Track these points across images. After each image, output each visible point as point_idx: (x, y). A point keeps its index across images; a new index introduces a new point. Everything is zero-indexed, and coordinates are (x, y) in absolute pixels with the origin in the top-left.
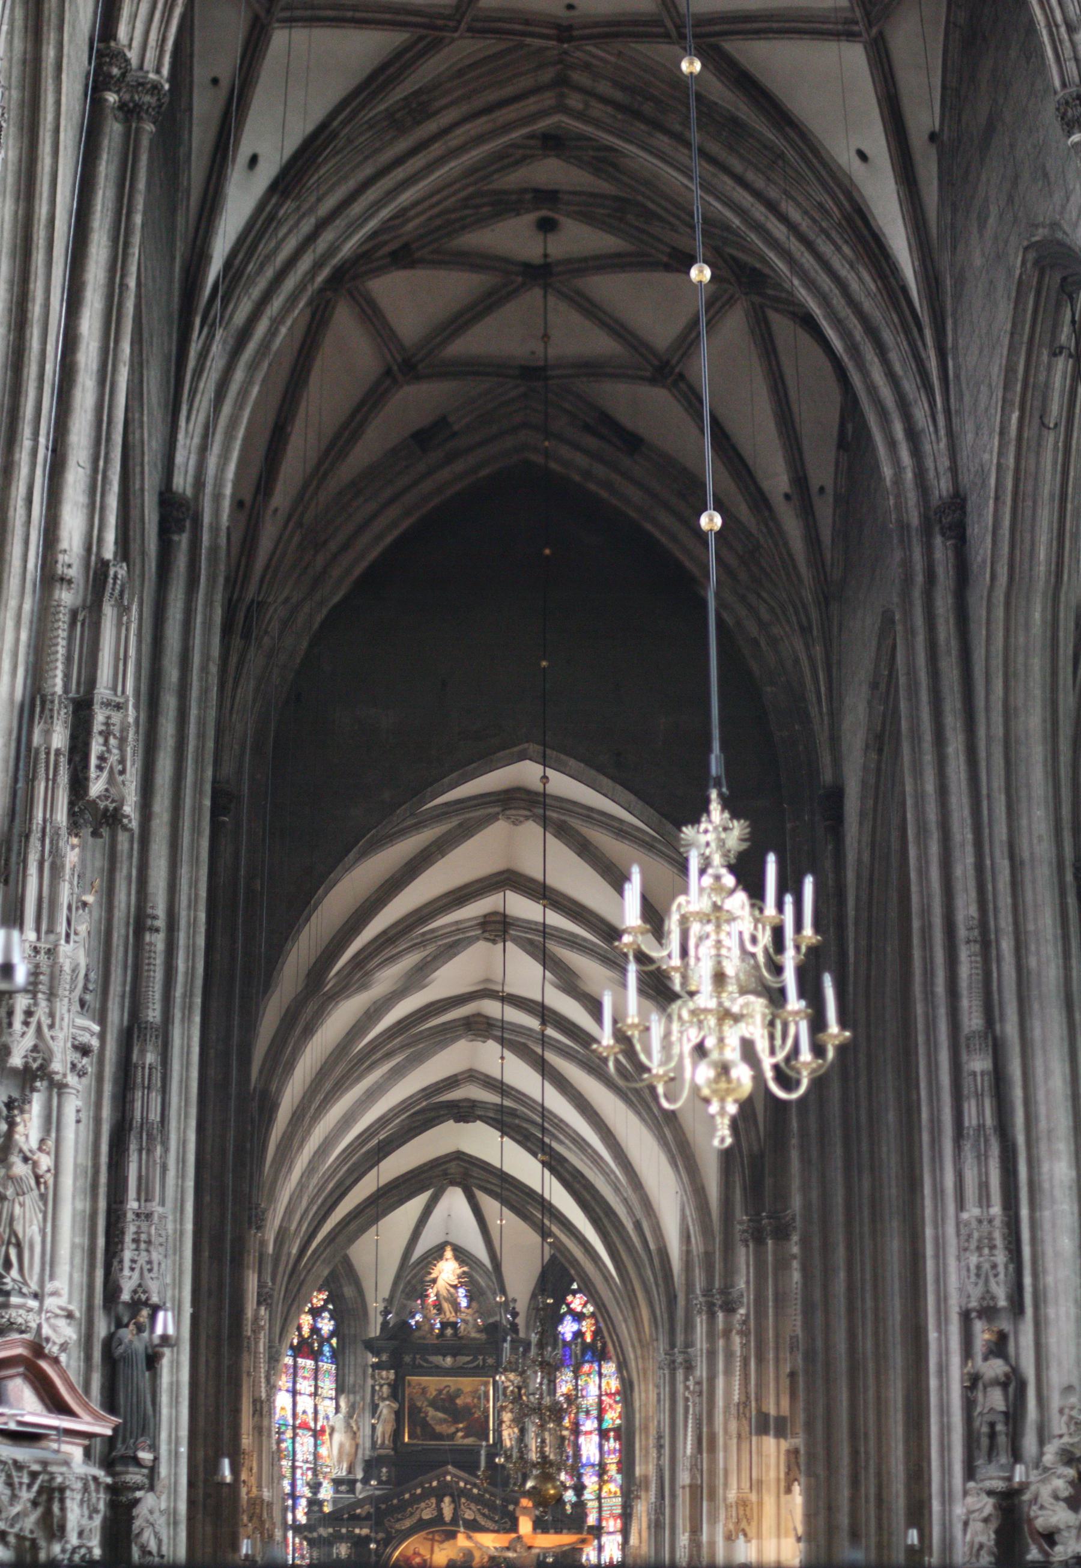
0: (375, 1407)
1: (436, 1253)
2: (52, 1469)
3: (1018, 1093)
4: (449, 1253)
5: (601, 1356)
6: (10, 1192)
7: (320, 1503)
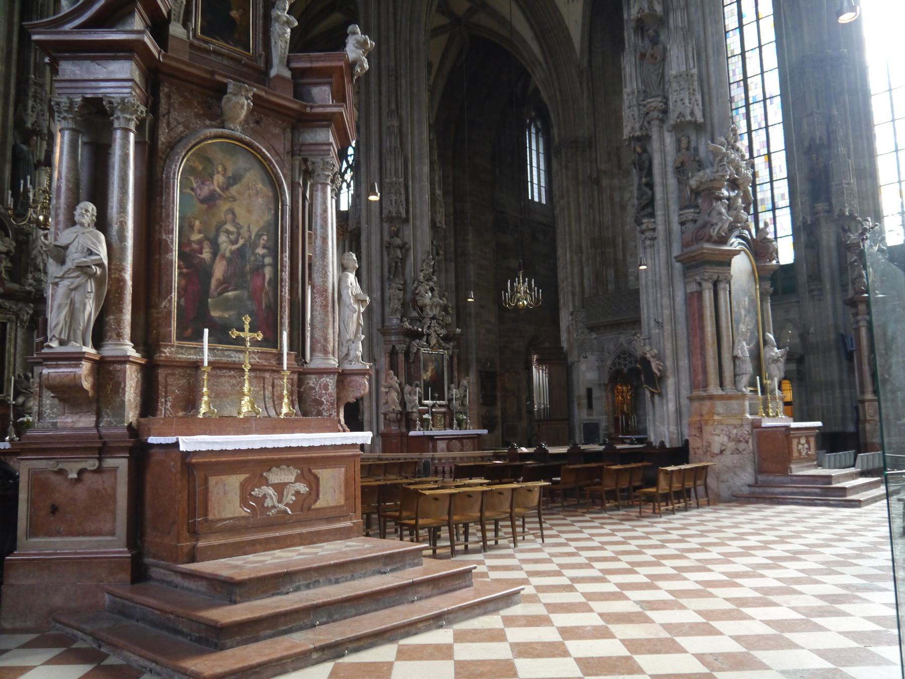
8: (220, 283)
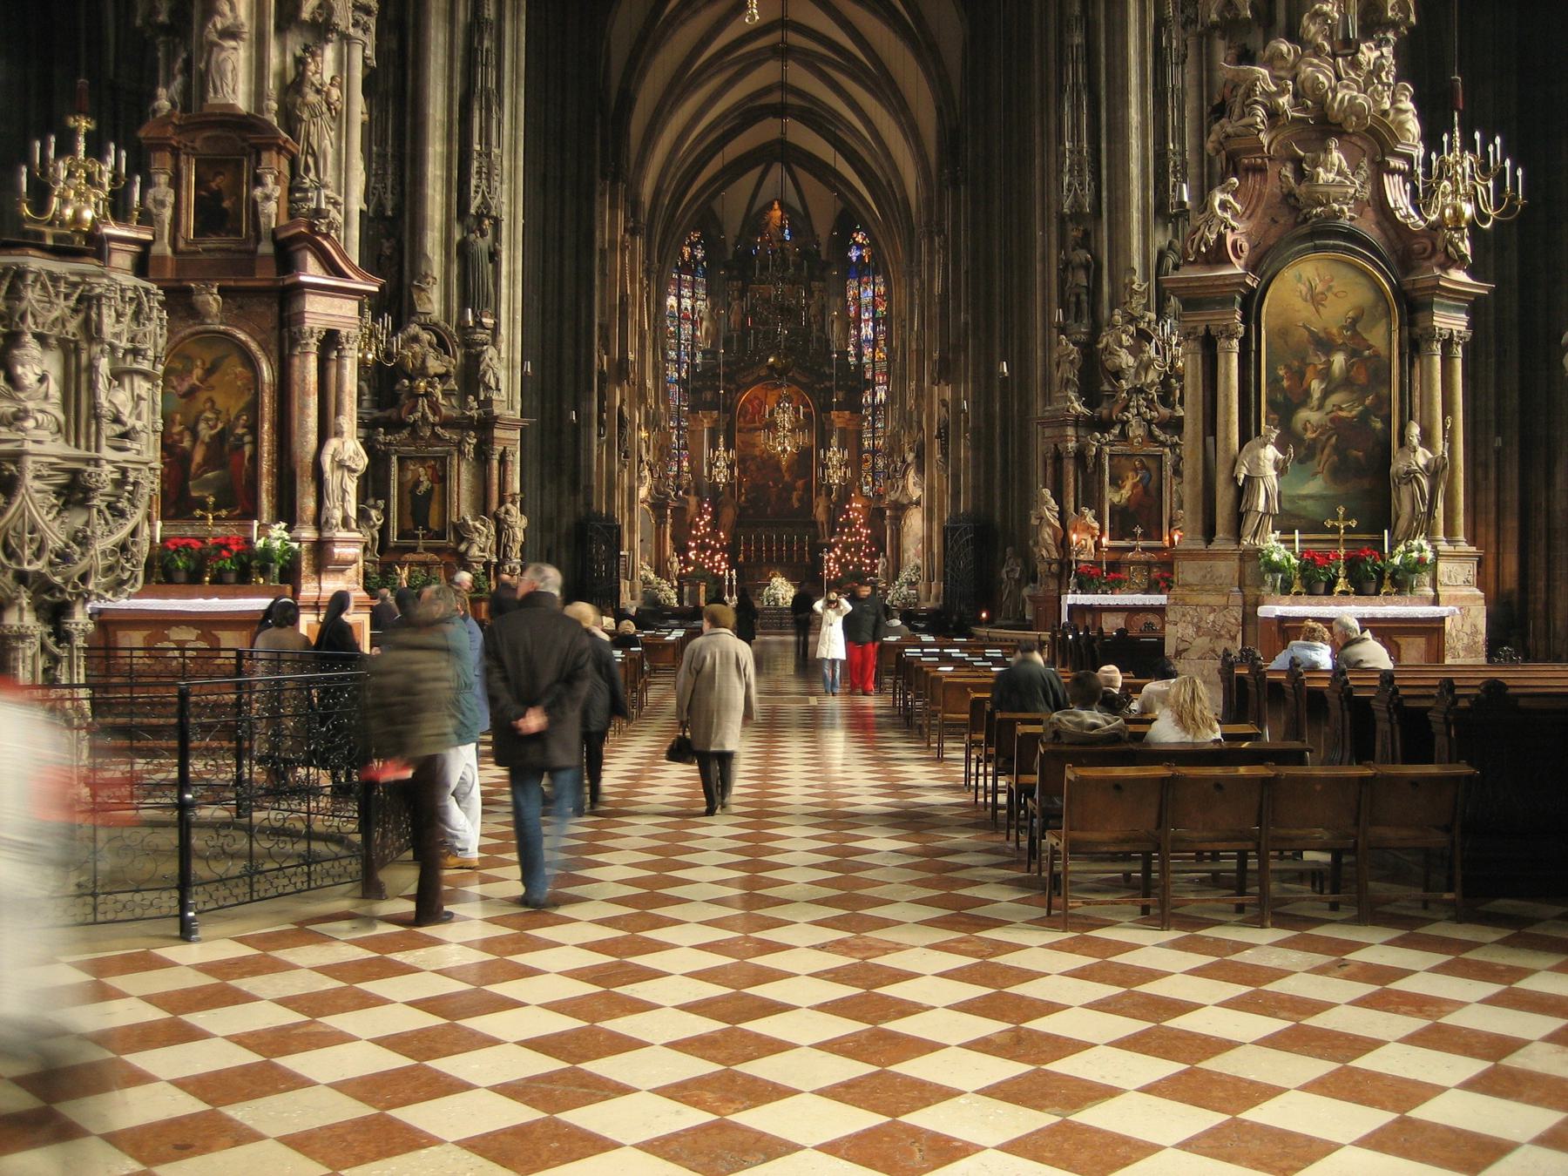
0: (729, 305)
1: (770, 206)
2: (93, 280)
3: (1103, 59)
4: (776, 206)
5: (876, 272)
6: (305, 116)
7: (694, 366)
8: (200, 466)
